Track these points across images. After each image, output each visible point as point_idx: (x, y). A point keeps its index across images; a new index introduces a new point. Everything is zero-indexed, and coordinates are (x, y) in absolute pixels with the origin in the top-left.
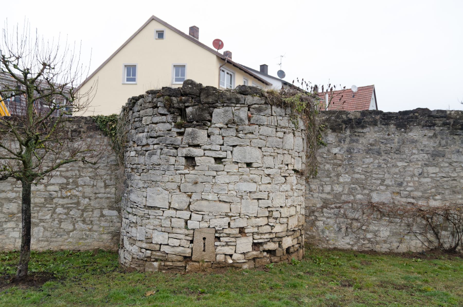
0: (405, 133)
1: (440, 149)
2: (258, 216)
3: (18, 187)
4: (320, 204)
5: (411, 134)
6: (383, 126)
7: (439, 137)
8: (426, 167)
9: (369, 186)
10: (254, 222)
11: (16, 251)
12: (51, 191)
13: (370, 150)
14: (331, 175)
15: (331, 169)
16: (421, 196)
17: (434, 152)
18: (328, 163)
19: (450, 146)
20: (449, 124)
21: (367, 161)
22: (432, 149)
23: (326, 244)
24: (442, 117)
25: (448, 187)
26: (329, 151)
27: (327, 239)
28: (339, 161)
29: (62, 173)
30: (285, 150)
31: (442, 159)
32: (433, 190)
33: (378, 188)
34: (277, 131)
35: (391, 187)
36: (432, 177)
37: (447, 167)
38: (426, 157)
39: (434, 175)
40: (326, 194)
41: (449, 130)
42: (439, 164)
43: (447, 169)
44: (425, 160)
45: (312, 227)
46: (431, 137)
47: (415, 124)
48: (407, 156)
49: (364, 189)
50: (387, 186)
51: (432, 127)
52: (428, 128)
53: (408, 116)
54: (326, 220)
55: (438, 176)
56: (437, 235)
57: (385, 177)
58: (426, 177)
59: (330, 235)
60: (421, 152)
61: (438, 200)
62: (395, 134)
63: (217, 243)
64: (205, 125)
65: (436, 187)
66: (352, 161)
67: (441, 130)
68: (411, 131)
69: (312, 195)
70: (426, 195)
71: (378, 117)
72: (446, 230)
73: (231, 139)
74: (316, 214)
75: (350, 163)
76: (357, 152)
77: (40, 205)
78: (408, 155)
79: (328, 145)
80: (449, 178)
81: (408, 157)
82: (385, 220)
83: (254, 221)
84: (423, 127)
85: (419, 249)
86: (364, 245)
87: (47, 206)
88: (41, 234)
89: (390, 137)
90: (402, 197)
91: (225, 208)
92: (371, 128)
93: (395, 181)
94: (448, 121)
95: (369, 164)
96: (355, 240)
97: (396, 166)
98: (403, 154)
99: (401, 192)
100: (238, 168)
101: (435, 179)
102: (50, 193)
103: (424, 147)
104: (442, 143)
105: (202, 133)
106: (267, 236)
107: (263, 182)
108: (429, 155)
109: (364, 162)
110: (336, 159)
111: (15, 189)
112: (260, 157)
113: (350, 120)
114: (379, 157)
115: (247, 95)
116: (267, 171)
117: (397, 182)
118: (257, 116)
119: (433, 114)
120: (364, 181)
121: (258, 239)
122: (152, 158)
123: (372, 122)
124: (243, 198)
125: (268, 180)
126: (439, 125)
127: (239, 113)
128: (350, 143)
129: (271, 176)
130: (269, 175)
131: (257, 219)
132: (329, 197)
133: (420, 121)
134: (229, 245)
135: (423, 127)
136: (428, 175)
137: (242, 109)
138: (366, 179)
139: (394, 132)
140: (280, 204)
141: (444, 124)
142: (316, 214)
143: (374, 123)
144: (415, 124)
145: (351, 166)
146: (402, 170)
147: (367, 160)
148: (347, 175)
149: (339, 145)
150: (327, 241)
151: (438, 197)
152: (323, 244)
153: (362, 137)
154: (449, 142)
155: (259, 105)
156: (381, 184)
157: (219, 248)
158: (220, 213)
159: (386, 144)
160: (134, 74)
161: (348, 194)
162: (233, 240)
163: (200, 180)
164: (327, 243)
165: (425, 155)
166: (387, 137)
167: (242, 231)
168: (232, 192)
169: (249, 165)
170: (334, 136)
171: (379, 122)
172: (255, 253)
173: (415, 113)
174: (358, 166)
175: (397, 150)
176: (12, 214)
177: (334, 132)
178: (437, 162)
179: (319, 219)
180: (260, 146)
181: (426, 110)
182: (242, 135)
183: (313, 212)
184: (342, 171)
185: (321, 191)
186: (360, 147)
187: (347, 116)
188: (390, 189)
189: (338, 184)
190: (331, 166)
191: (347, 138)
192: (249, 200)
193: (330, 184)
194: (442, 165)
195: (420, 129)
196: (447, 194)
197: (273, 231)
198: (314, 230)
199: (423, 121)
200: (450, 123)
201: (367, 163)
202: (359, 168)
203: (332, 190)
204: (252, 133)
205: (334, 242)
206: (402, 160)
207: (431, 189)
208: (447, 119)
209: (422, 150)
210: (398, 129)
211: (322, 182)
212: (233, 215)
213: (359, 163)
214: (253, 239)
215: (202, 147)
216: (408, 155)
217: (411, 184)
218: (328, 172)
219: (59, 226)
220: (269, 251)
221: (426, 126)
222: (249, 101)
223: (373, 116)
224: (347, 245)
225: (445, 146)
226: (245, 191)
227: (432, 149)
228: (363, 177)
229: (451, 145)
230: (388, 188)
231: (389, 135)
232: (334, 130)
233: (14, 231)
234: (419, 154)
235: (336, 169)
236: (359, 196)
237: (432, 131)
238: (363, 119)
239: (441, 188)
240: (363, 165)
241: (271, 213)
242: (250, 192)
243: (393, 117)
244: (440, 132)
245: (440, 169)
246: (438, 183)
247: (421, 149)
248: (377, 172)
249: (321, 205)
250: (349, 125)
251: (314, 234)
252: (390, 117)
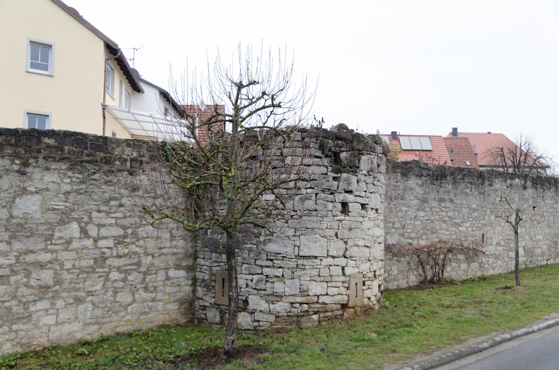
3: (55, 244)
5: (410, 182)
7: (425, 185)
12: (102, 248)
22: (422, 196)
29: (118, 221)
36: (421, 220)
46: (420, 186)
50: (396, 229)
63: (364, 288)
77: (87, 270)
87: (98, 270)
88: (89, 314)
89: (397, 184)
97: (401, 211)
102: (102, 250)
105: (354, 179)
111: (49, 247)
122: (305, 203)
141: (428, 175)
146: (405, 214)
160: (46, 58)
163: (353, 226)
176: (44, 288)
206: (405, 205)
217: (410, 227)
219: (113, 298)
233: (47, 314)
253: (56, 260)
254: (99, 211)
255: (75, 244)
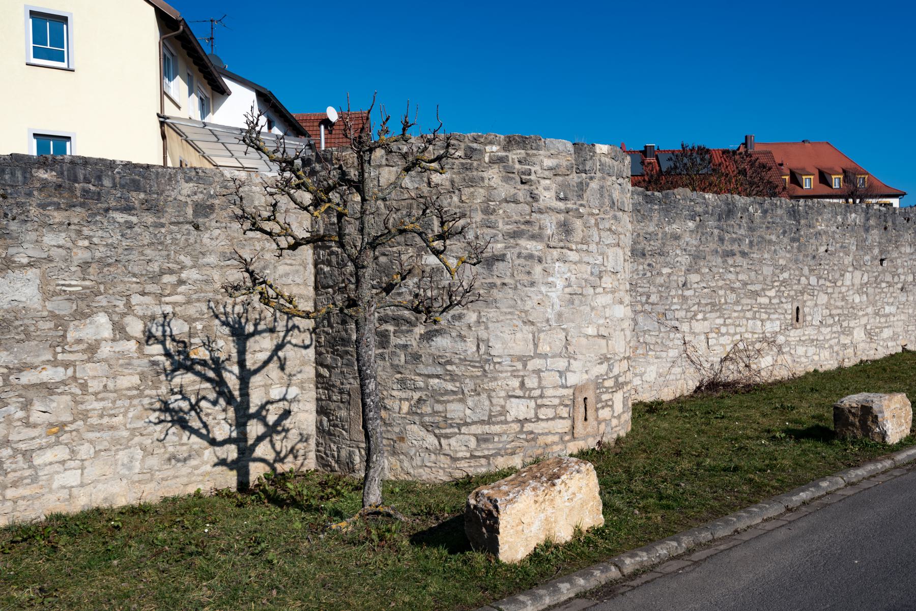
3: (70, 352)
12: (153, 356)
22: (694, 248)
29: (178, 309)
77: (130, 393)
87: (147, 392)
97: (660, 274)
102: (152, 359)
111: (60, 357)
122: (495, 267)
146: (667, 280)
160: (58, 40)
176: (57, 426)
206: (667, 265)
217: (675, 300)
219: (177, 438)
233: (65, 470)
253: (74, 378)
254: (143, 294)
255: (105, 350)
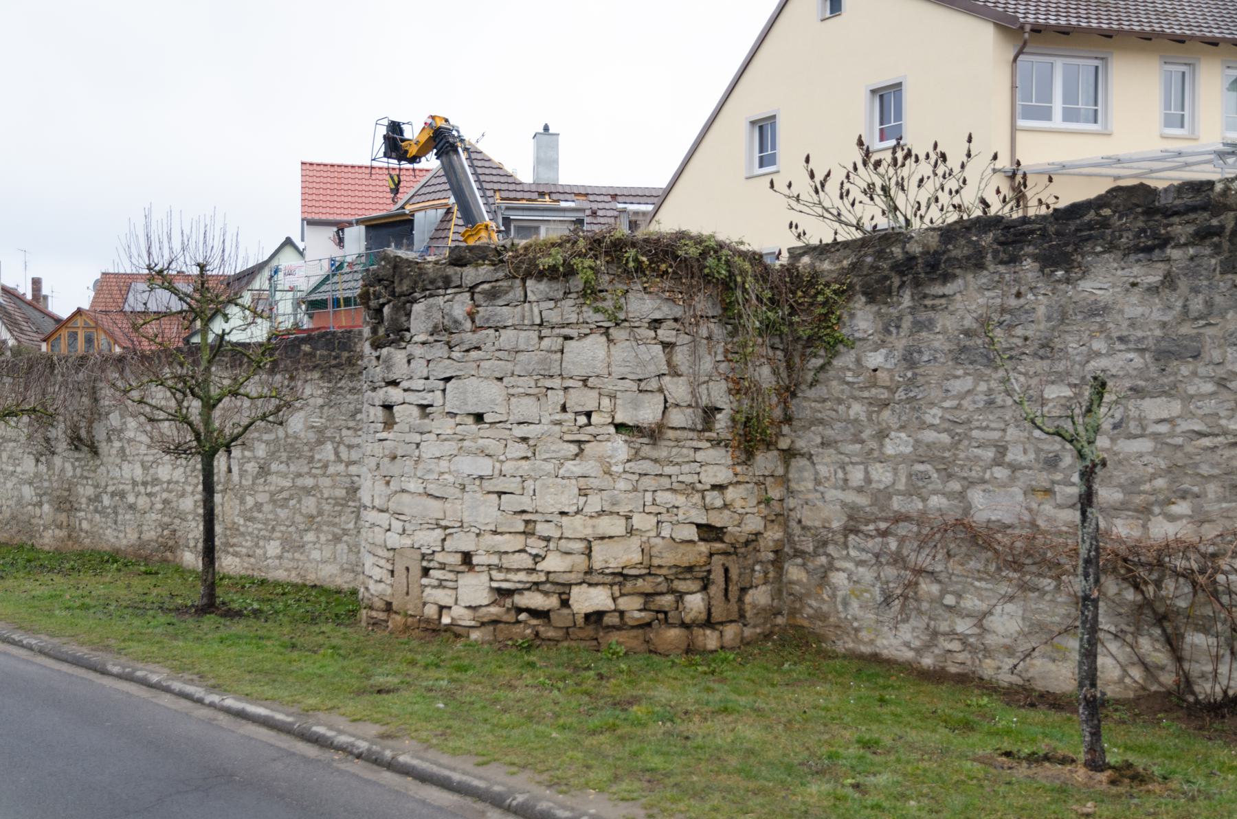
0: (1068, 281)
1: (1186, 329)
2: (499, 530)
4: (839, 521)
5: (1086, 285)
6: (1002, 269)
7: (1183, 285)
8: (1136, 399)
9: (962, 467)
10: (489, 543)
11: (315, 586)
13: (963, 349)
14: (864, 436)
15: (863, 417)
16: (1122, 503)
17: (1163, 344)
18: (855, 398)
19: (1222, 315)
20: (1219, 231)
21: (958, 386)
22: (1158, 333)
23: (853, 642)
24: (1193, 209)
25: (1216, 471)
26: (858, 361)
27: (856, 624)
28: (882, 390)
30: (571, 378)
31: (1191, 367)
32: (1160, 483)
33: (987, 476)
34: (541, 338)
35: (1026, 471)
36: (1156, 436)
37: (1213, 394)
38: (1138, 361)
39: (1163, 428)
40: (855, 493)
41: (1218, 254)
42: (1181, 387)
43: (1210, 405)
44: (1135, 373)
45: (821, 589)
46: (1153, 290)
47: (1099, 249)
48: (1074, 362)
49: (950, 476)
50: (1014, 468)
51: (1157, 251)
52: (1141, 255)
53: (1078, 222)
54: (853, 569)
55: (1178, 430)
56: (1173, 644)
57: (1007, 438)
58: (1136, 437)
59: (862, 613)
60: (1119, 346)
61: (1180, 517)
62: (1035, 291)
63: (425, 581)
64: (402, 339)
65: (1172, 470)
66: (917, 390)
67: (1192, 259)
68: (1085, 274)
69: (822, 493)
70: (1138, 500)
71: (988, 239)
72: (1206, 631)
73: (441, 365)
74: (831, 549)
75: (912, 394)
76: (929, 361)
78: (1078, 358)
79: (858, 344)
80: (1220, 439)
81: (1077, 367)
82: (1010, 580)
83: (490, 540)
84: (1125, 255)
85: (1112, 687)
86: (949, 655)
87: (350, 503)
88: (345, 557)
89: (1022, 301)
90: (1059, 506)
91: (434, 509)
92: (970, 277)
93: (1038, 451)
94: (1215, 222)
95: (962, 396)
96: (923, 638)
98: (1060, 359)
99: (1057, 488)
100: (454, 426)
101: (1169, 441)
103: (1129, 326)
104: (1191, 307)
105: (399, 356)
106: (522, 576)
107: (509, 456)
108: (1147, 355)
109: (948, 391)
110: (875, 385)
112: (500, 400)
113: (911, 259)
114: (988, 371)
115: (465, 265)
116: (520, 431)
117: (1043, 455)
118: (489, 308)
119: (1163, 202)
120: (949, 451)
121: (502, 581)
123: (968, 258)
124: (467, 489)
125: (522, 449)
126: (1182, 241)
127: (451, 306)
128: (911, 332)
129: (531, 442)
130: (524, 439)
131: (498, 537)
132: (862, 501)
133: (1117, 234)
134: (445, 587)
135: (1125, 255)
136: (1144, 429)
137: (458, 297)
138: (955, 445)
139: (1033, 284)
140: (560, 506)
141: (1203, 235)
142: (831, 549)
143: (976, 263)
144: (1099, 249)
145: (914, 404)
147: (958, 383)
148: (903, 435)
149: (883, 341)
150: (857, 630)
151: (1182, 508)
152: (846, 638)
153: (942, 310)
154: (1218, 299)
155: (493, 284)
156: (998, 462)
157: (428, 590)
158: (427, 519)
159: (1011, 327)
161: (908, 494)
162: (451, 576)
163: (399, 453)
164: (856, 636)
165: (1131, 355)
166: (1013, 302)
167: (467, 558)
168: (446, 476)
169: (479, 418)
170: (871, 317)
171: (989, 256)
172: (494, 610)
173: (1101, 207)
174: (932, 404)
175: (1043, 346)
177: (870, 302)
178: (1172, 378)
179: (838, 564)
180: (499, 376)
181: (1143, 191)
182: (459, 355)
183: (825, 543)
184: (894, 422)
185: (841, 483)
186: (936, 344)
187: (903, 248)
188: (1024, 478)
189: (882, 462)
190: (864, 408)
191: (905, 319)
192: (478, 495)
193: (862, 463)
194: (1192, 390)
195: (1116, 265)
196: (1211, 496)
197: (539, 567)
198: (825, 596)
199: (1125, 235)
200: (1222, 227)
201: (955, 393)
202: (935, 411)
203: (868, 481)
204: (478, 348)
205: (873, 637)
207: (1153, 477)
208: (1213, 215)
209: (1122, 339)
210: (1047, 270)
211: (843, 457)
212: (449, 524)
213: (935, 394)
214: (491, 580)
215: (401, 385)
216: (1078, 358)
218: (856, 425)
220: (534, 613)
221: (1137, 249)
222: (469, 278)
223: (974, 238)
224: (904, 649)
225: (1202, 318)
226: (469, 475)
227: (1158, 333)
228: (945, 438)
229: (1226, 311)
230: (1018, 474)
231: (1018, 295)
232: (871, 298)
234: (1111, 353)
235: (874, 416)
236: (935, 501)
237: (1160, 265)
238: (944, 252)
239: (1190, 476)
240: (945, 399)
241: (531, 526)
242: (481, 478)
243: (1032, 232)
244: (1187, 267)
245: (1184, 407)
246: (1180, 454)
247: (1118, 334)
248: (983, 420)
249: (842, 523)
250: (910, 276)
251: (825, 608)
252: (1022, 234)
253: (317, 485)
254: (349, 429)
255: (331, 470)
